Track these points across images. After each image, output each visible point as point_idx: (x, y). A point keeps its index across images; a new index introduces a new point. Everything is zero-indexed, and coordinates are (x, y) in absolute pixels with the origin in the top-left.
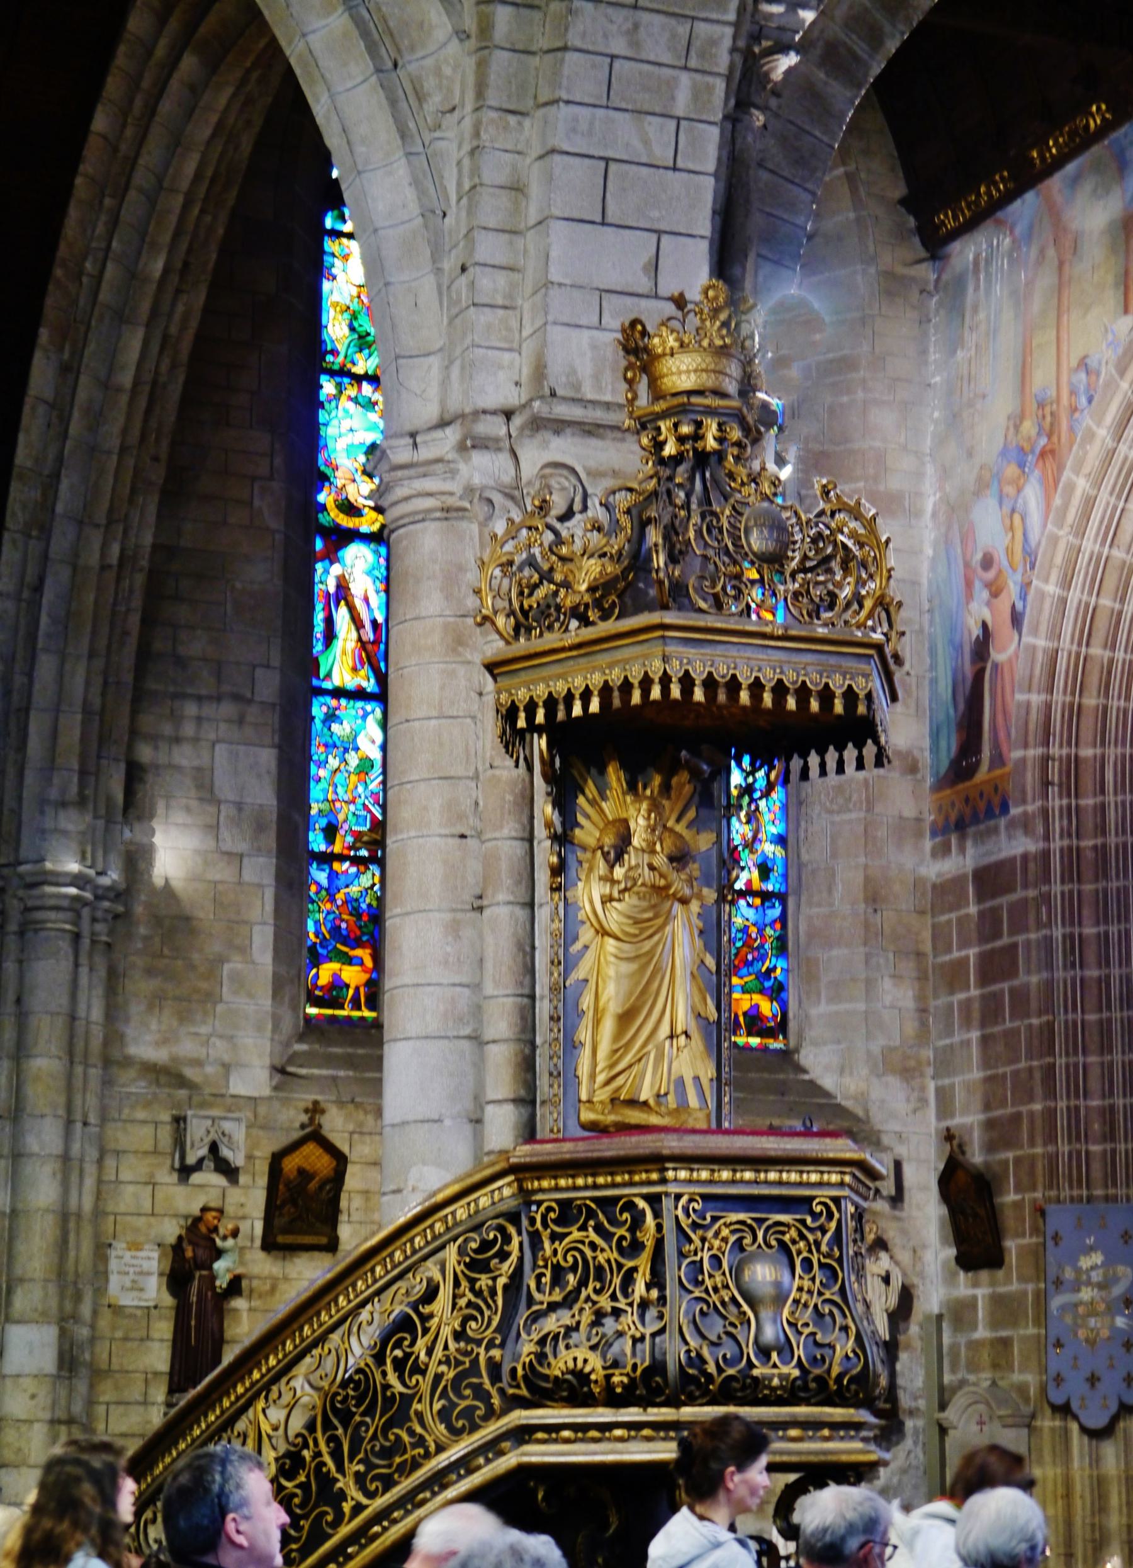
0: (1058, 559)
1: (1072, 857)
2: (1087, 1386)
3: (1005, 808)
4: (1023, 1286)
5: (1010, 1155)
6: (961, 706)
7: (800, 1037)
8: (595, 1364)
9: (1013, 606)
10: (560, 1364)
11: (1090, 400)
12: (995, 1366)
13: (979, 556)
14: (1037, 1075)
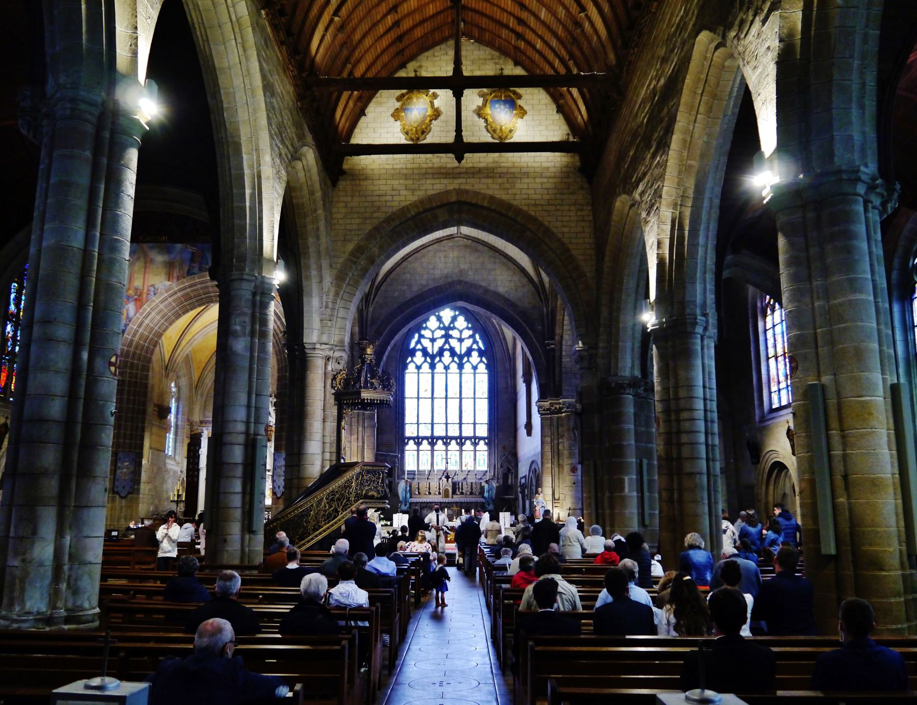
1: (130, 382)
8: (375, 494)
10: (370, 493)
11: (155, 294)
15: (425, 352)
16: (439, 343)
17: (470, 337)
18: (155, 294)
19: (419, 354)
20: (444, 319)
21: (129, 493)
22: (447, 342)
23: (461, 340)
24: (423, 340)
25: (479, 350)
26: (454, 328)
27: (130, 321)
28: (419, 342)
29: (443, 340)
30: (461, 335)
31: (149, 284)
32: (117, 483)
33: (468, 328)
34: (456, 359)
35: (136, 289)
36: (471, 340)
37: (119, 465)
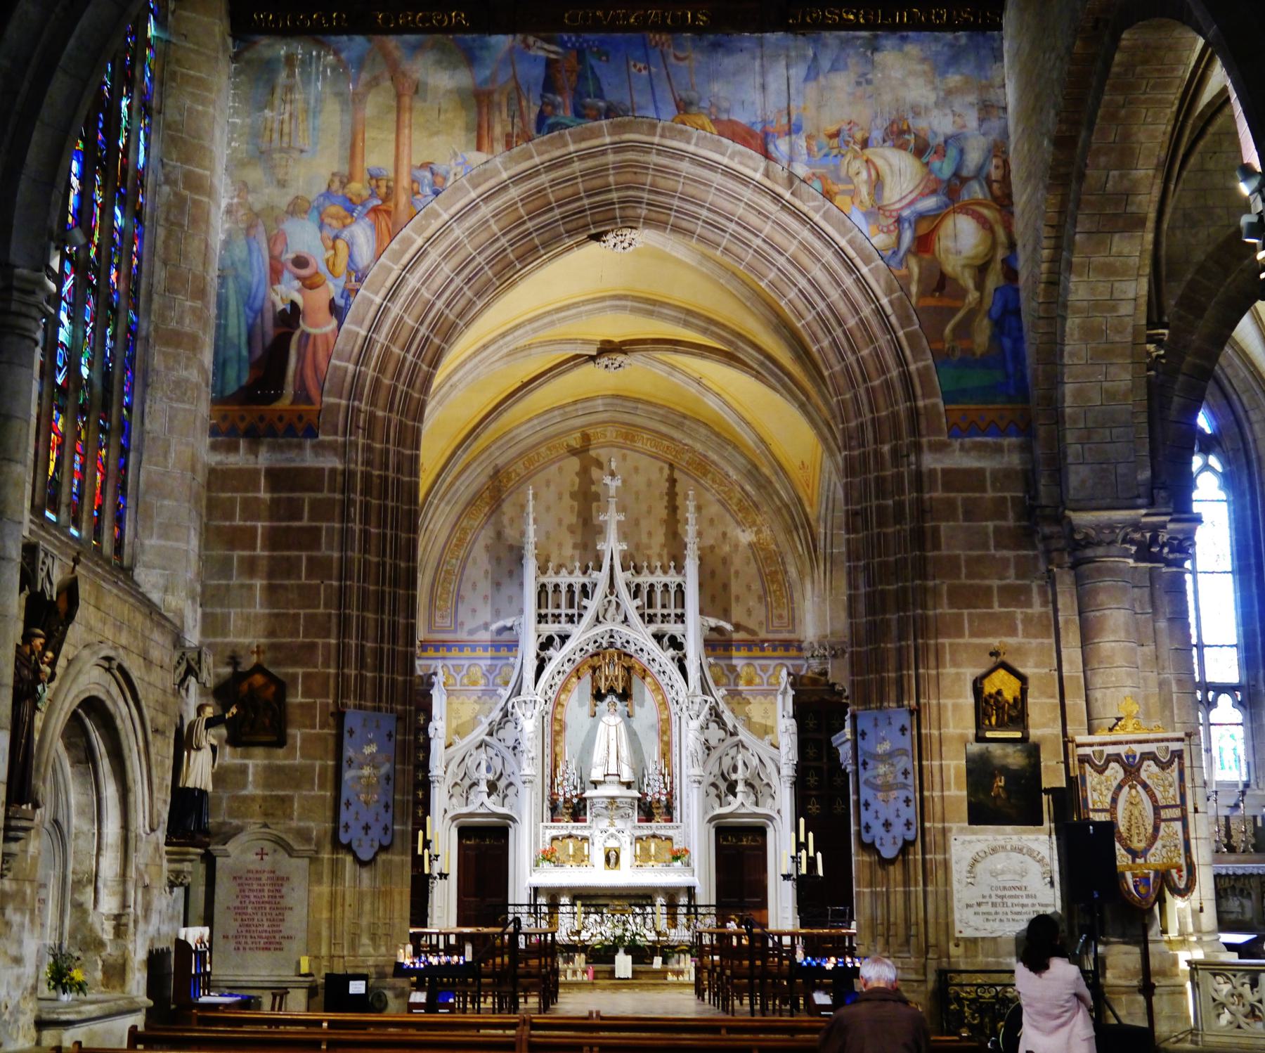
0: (389, 283)
2: (363, 832)
3: (311, 432)
4: (308, 762)
5: (300, 671)
6: (258, 352)
7: (134, 558)
9: (332, 301)
12: (266, 814)
13: (291, 256)
14: (334, 620)
18: (437, 193)
21: (383, 849)
27: (360, 280)
31: (417, 161)
32: (345, 816)
35: (374, 177)
37: (349, 752)
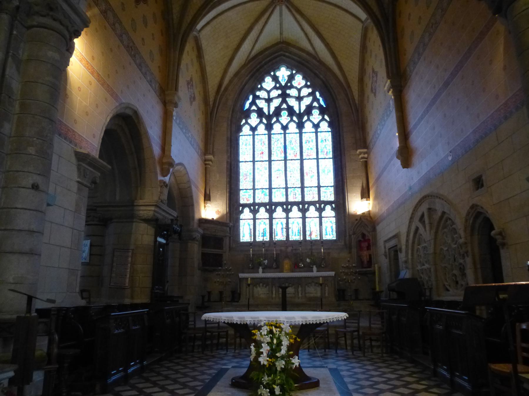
15: (260, 113)
16: (276, 103)
17: (309, 95)
19: (254, 116)
20: (280, 79)
22: (284, 101)
23: (299, 99)
24: (258, 102)
25: (320, 108)
26: (292, 87)
28: (253, 103)
29: (280, 99)
30: (299, 93)
33: (306, 86)
34: (295, 118)
36: (310, 99)
